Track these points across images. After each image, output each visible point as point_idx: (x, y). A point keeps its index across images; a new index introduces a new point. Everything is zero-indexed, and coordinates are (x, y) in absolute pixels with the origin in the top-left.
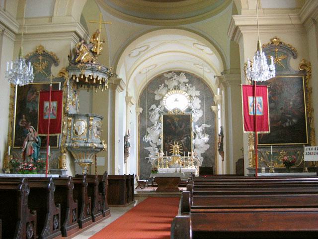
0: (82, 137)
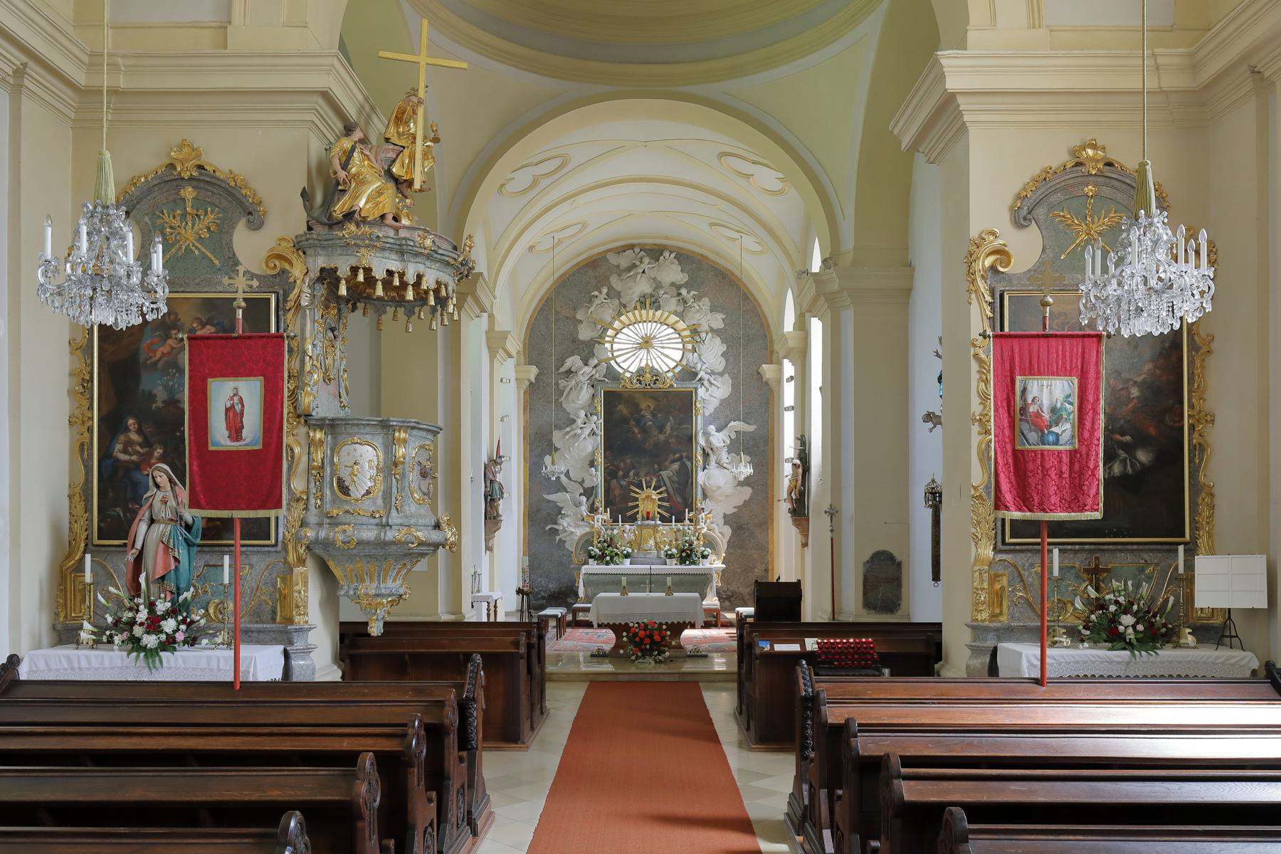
0: (368, 506)
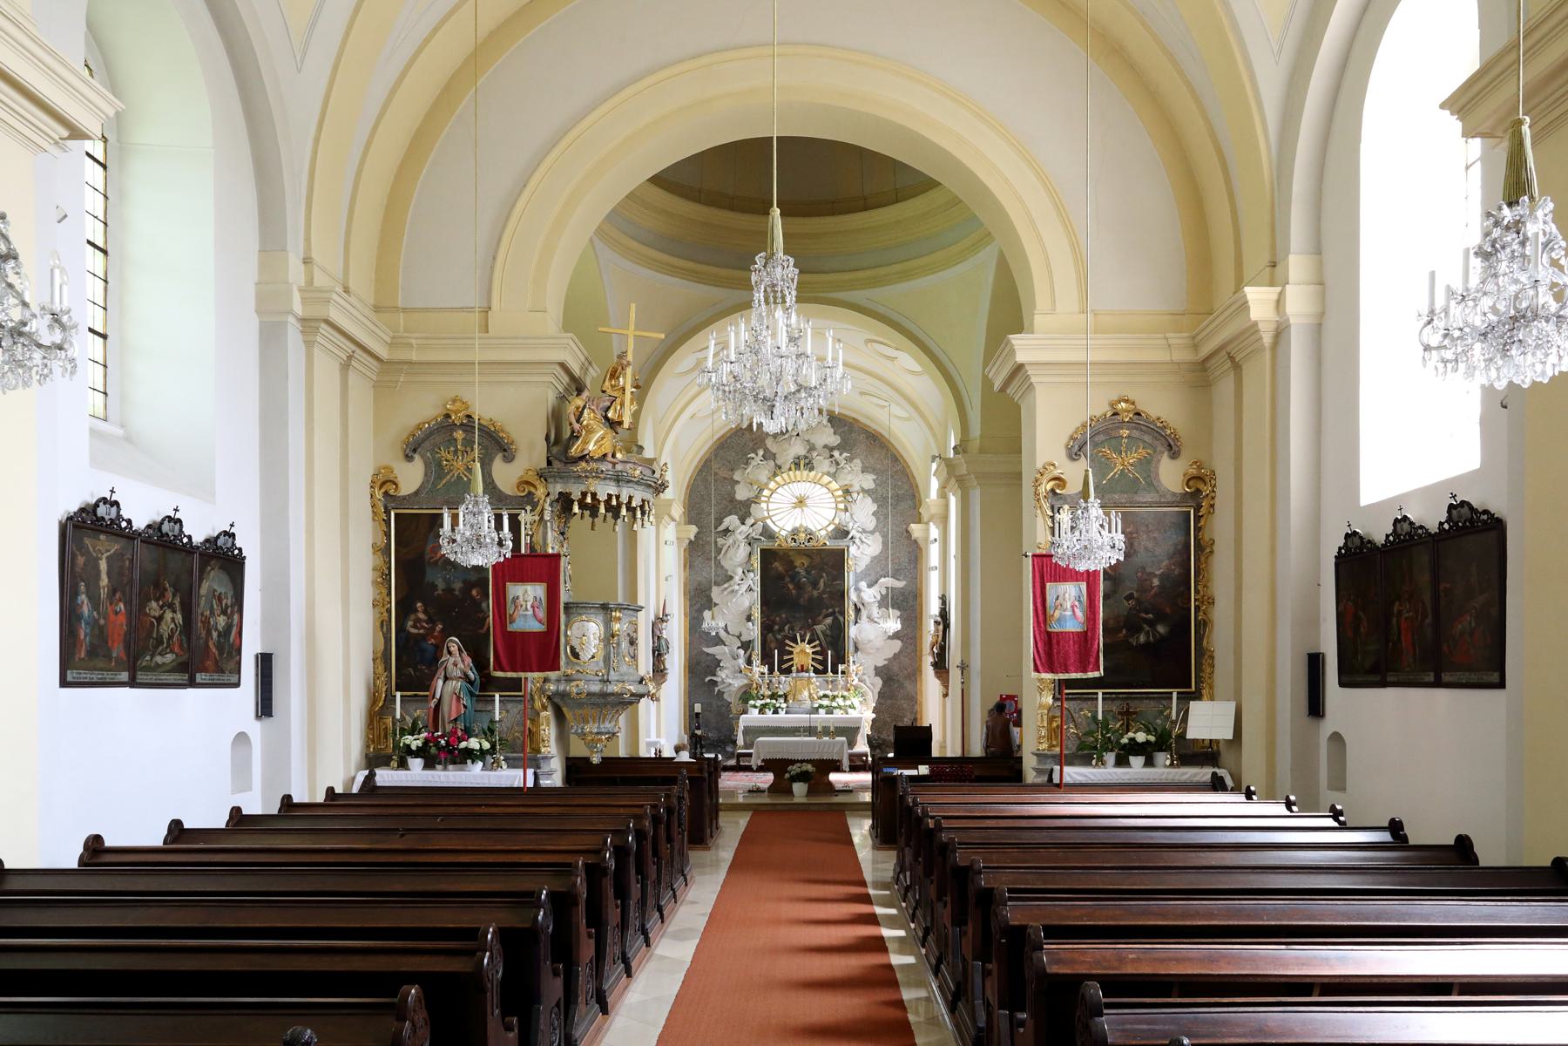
0: (591, 668)
